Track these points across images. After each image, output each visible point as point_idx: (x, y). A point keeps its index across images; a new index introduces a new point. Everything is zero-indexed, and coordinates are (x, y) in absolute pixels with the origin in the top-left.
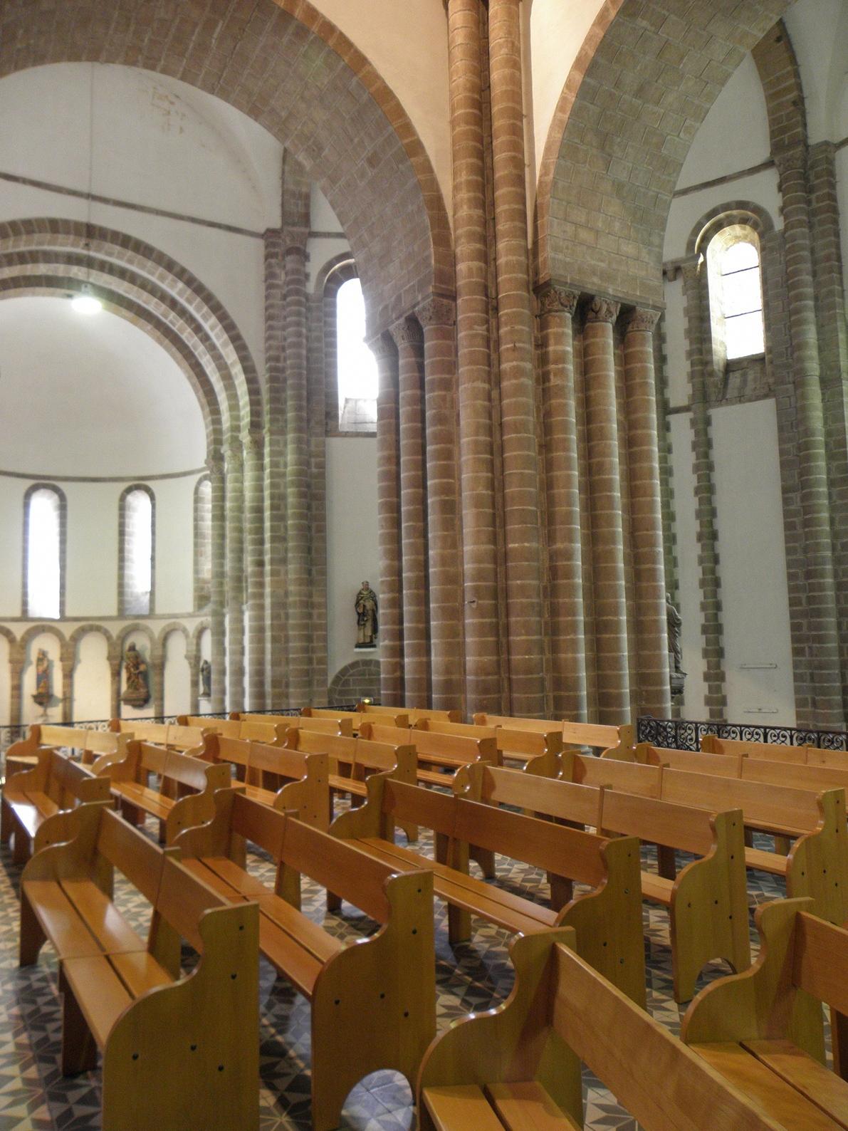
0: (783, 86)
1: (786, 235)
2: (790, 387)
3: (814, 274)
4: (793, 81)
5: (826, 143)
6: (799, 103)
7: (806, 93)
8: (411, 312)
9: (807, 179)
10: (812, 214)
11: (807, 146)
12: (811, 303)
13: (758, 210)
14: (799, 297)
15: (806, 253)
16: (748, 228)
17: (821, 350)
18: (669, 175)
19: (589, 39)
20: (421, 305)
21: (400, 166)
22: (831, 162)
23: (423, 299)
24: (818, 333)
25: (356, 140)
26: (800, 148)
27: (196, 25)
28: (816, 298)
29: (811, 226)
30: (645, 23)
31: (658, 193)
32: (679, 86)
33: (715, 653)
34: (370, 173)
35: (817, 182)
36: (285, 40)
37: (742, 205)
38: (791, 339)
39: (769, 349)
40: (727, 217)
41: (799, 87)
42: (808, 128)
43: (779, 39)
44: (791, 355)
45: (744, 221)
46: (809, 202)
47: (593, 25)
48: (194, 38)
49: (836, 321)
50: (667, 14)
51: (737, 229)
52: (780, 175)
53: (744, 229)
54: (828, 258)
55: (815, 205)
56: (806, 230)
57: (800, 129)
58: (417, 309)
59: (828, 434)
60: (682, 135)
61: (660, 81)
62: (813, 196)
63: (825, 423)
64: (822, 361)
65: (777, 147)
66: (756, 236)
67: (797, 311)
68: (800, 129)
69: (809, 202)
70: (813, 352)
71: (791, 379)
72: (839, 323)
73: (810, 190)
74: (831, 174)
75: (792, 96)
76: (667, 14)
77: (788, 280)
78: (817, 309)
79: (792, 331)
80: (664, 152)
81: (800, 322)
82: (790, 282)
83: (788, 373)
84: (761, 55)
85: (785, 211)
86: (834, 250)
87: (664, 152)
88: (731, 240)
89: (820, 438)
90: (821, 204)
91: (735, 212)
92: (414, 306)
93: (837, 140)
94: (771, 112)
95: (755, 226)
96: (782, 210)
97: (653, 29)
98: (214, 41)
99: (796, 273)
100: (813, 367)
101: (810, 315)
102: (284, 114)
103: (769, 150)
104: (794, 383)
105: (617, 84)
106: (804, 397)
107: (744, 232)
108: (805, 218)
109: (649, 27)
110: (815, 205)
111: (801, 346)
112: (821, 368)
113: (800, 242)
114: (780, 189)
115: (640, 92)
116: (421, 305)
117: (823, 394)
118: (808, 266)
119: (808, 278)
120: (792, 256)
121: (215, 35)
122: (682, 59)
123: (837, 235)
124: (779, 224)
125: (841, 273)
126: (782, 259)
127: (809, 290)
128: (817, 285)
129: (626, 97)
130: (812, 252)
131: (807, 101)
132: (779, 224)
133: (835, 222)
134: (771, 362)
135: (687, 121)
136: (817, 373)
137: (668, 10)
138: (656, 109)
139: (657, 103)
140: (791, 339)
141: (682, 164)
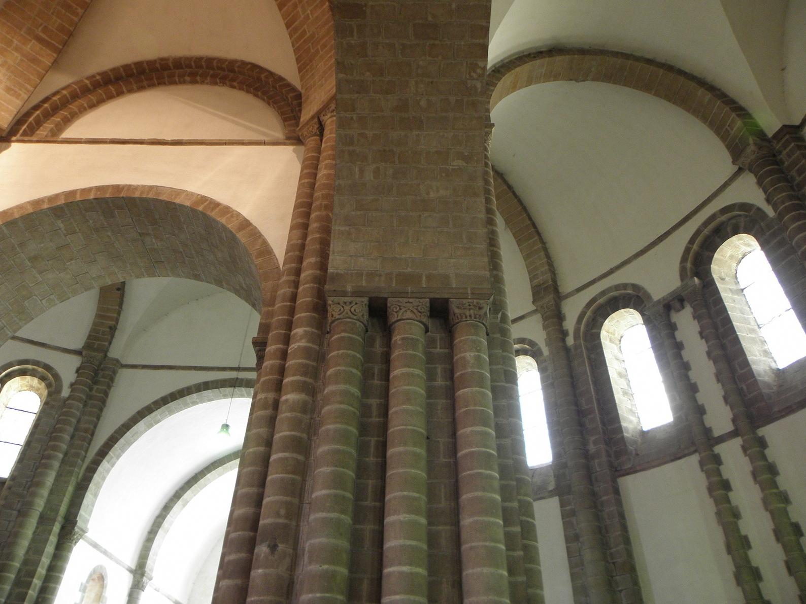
0: (109, 314)
1: (67, 402)
2: (15, 513)
3: (72, 437)
4: (115, 315)
5: (117, 361)
6: (113, 329)
7: (119, 326)
9: (96, 374)
10: (90, 397)
11: (106, 356)
12: (61, 456)
13: (56, 376)
14: (55, 448)
15: (74, 421)
16: (43, 384)
17: (51, 492)
18: (20, 320)
19: (20, 207)
22: (115, 372)
24: (56, 479)
26: (101, 355)
28: (66, 454)
29: (85, 405)
30: (61, 225)
31: (5, 326)
32: (60, 273)
35: (102, 380)
37: (47, 367)
38: (34, 476)
39: (13, 477)
40: (33, 370)
41: (117, 321)
42: (111, 346)
43: (118, 289)
44: (29, 488)
45: (42, 378)
46: (91, 389)
47: (29, 202)
49: (72, 475)
50: (78, 231)
51: (35, 382)
52: (82, 363)
53: (40, 384)
54: (86, 431)
55: (94, 393)
56: (81, 405)
57: (106, 344)
59: (25, 562)
60: (44, 301)
61: (50, 262)
62: (95, 387)
63: (27, 552)
64: (48, 502)
65: (88, 346)
66: (45, 392)
67: (49, 457)
68: (106, 344)
69: (91, 389)
70: (45, 492)
71: (19, 507)
72: (73, 478)
73: (95, 382)
74: (112, 380)
75: (112, 323)
76: (78, 231)
77: (53, 433)
78: (63, 462)
79: (39, 470)
80: (26, 304)
81: (47, 466)
82: (54, 434)
83: (19, 501)
84: (104, 292)
85: (73, 387)
86: (92, 427)
87: (26, 304)
88: (27, 386)
89: (17, 564)
90: (98, 395)
91: (40, 369)
93: (124, 362)
94: (94, 324)
95: (49, 386)
96: (72, 385)
97: (65, 232)
99: (61, 430)
100: (40, 504)
101: (56, 464)
103: (83, 345)
104: (19, 511)
105: (22, 245)
106: (22, 525)
107: (39, 386)
108: (84, 397)
109: (63, 229)
110: (94, 393)
111: (39, 484)
112: (45, 507)
113: (75, 411)
114: (77, 371)
115: (34, 259)
117: (37, 528)
118: (70, 429)
119: (67, 437)
120: (65, 418)
122: (72, 259)
123: (98, 418)
124: (66, 392)
125: (89, 444)
126: (56, 416)
127: (64, 447)
128: (71, 445)
129: (23, 255)
130: (79, 421)
131: (117, 331)
132: (66, 392)
133: (101, 410)
134: (10, 488)
135: (53, 296)
136: (40, 509)
137: (80, 230)
138: (38, 276)
139: (40, 273)
140: (34, 476)
141: (33, 319)
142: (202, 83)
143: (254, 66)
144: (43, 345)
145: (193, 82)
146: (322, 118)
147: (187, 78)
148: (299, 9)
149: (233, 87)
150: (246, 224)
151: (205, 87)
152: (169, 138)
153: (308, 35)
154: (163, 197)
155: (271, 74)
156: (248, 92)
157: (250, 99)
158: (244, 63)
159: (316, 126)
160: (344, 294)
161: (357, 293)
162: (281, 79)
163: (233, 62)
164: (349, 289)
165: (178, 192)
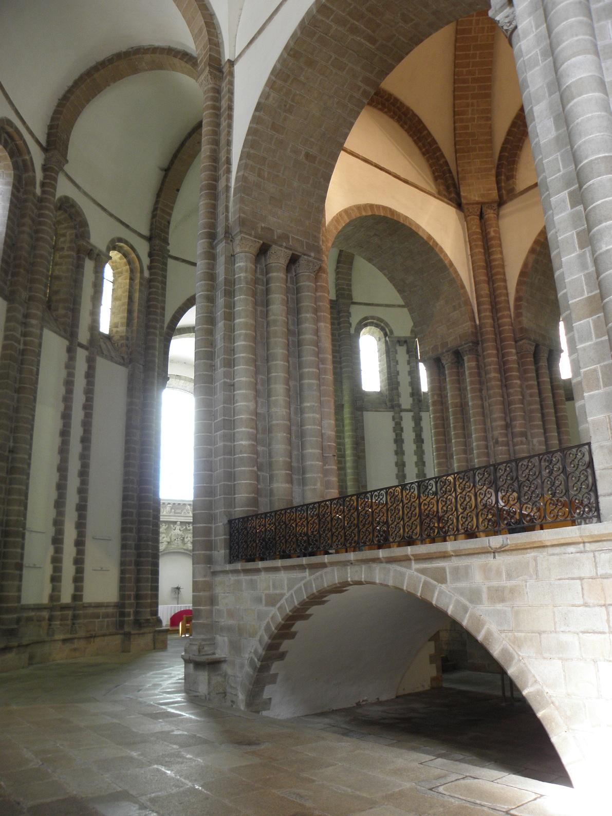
8: (299, 254)
20: (310, 259)
21: (322, 180)
23: (314, 258)
25: (312, 140)
27: (374, 31)
33: (81, 526)
34: (302, 157)
36: (360, 84)
47: (354, 206)
48: (362, 26)
58: (306, 257)
92: (304, 255)
98: (359, 38)
102: (302, 78)
116: (310, 259)
121: (362, 40)
142: (386, 113)
143: (420, 121)
144: (127, 226)
145: (381, 110)
146: (484, 209)
147: (380, 106)
148: (470, 109)
149: (402, 126)
150: (451, 264)
151: (385, 116)
152: (402, 176)
153: (470, 131)
154: (414, 228)
155: (429, 134)
156: (411, 136)
157: (409, 141)
158: (415, 115)
159: (480, 210)
160: (530, 339)
161: (534, 341)
162: (434, 141)
163: (408, 109)
164: (532, 338)
165: (418, 226)
